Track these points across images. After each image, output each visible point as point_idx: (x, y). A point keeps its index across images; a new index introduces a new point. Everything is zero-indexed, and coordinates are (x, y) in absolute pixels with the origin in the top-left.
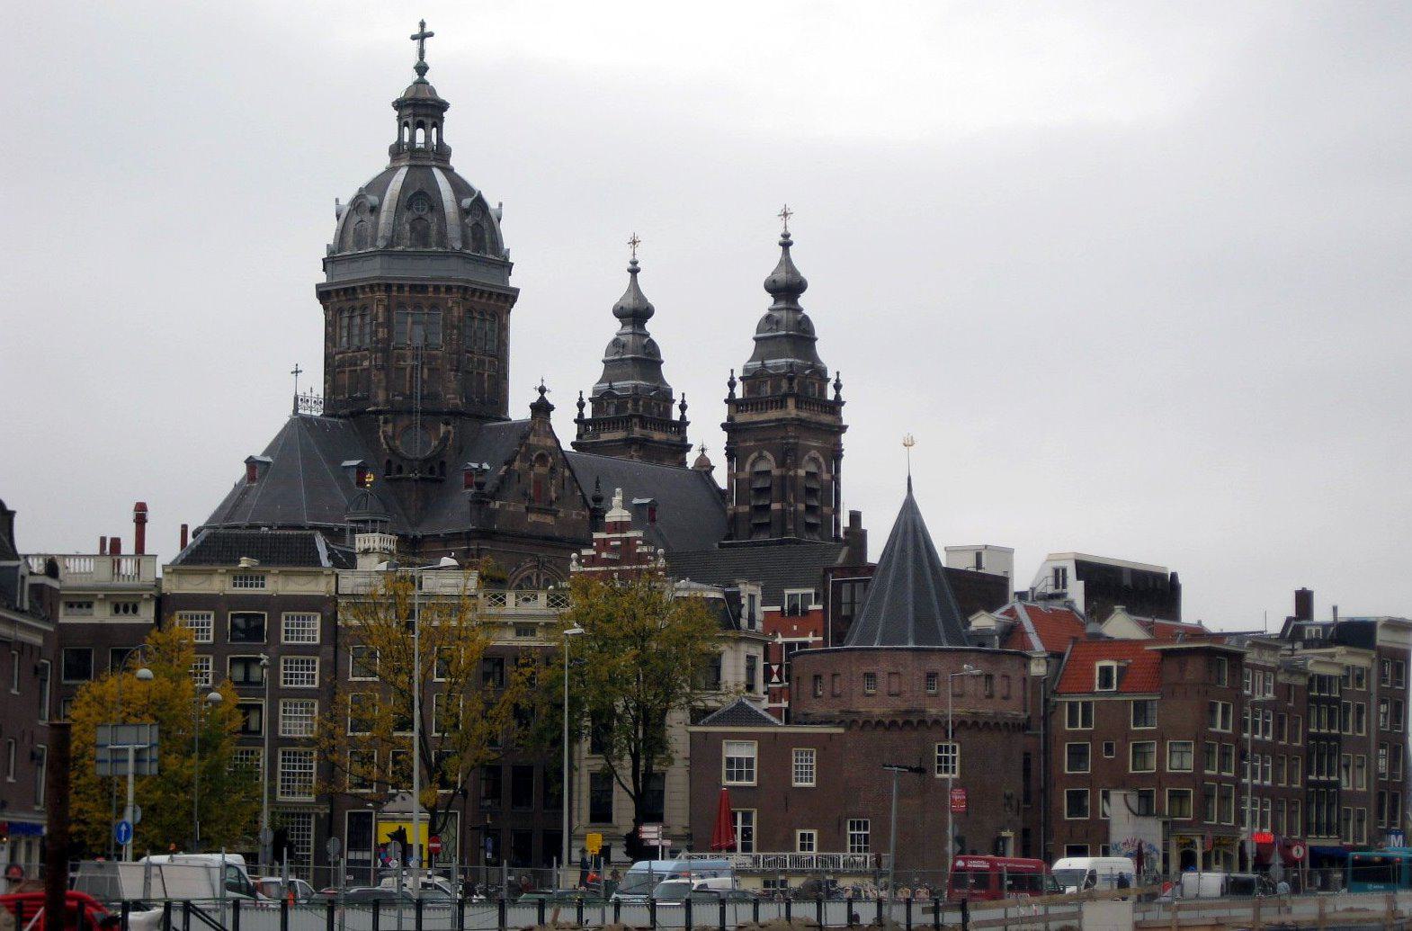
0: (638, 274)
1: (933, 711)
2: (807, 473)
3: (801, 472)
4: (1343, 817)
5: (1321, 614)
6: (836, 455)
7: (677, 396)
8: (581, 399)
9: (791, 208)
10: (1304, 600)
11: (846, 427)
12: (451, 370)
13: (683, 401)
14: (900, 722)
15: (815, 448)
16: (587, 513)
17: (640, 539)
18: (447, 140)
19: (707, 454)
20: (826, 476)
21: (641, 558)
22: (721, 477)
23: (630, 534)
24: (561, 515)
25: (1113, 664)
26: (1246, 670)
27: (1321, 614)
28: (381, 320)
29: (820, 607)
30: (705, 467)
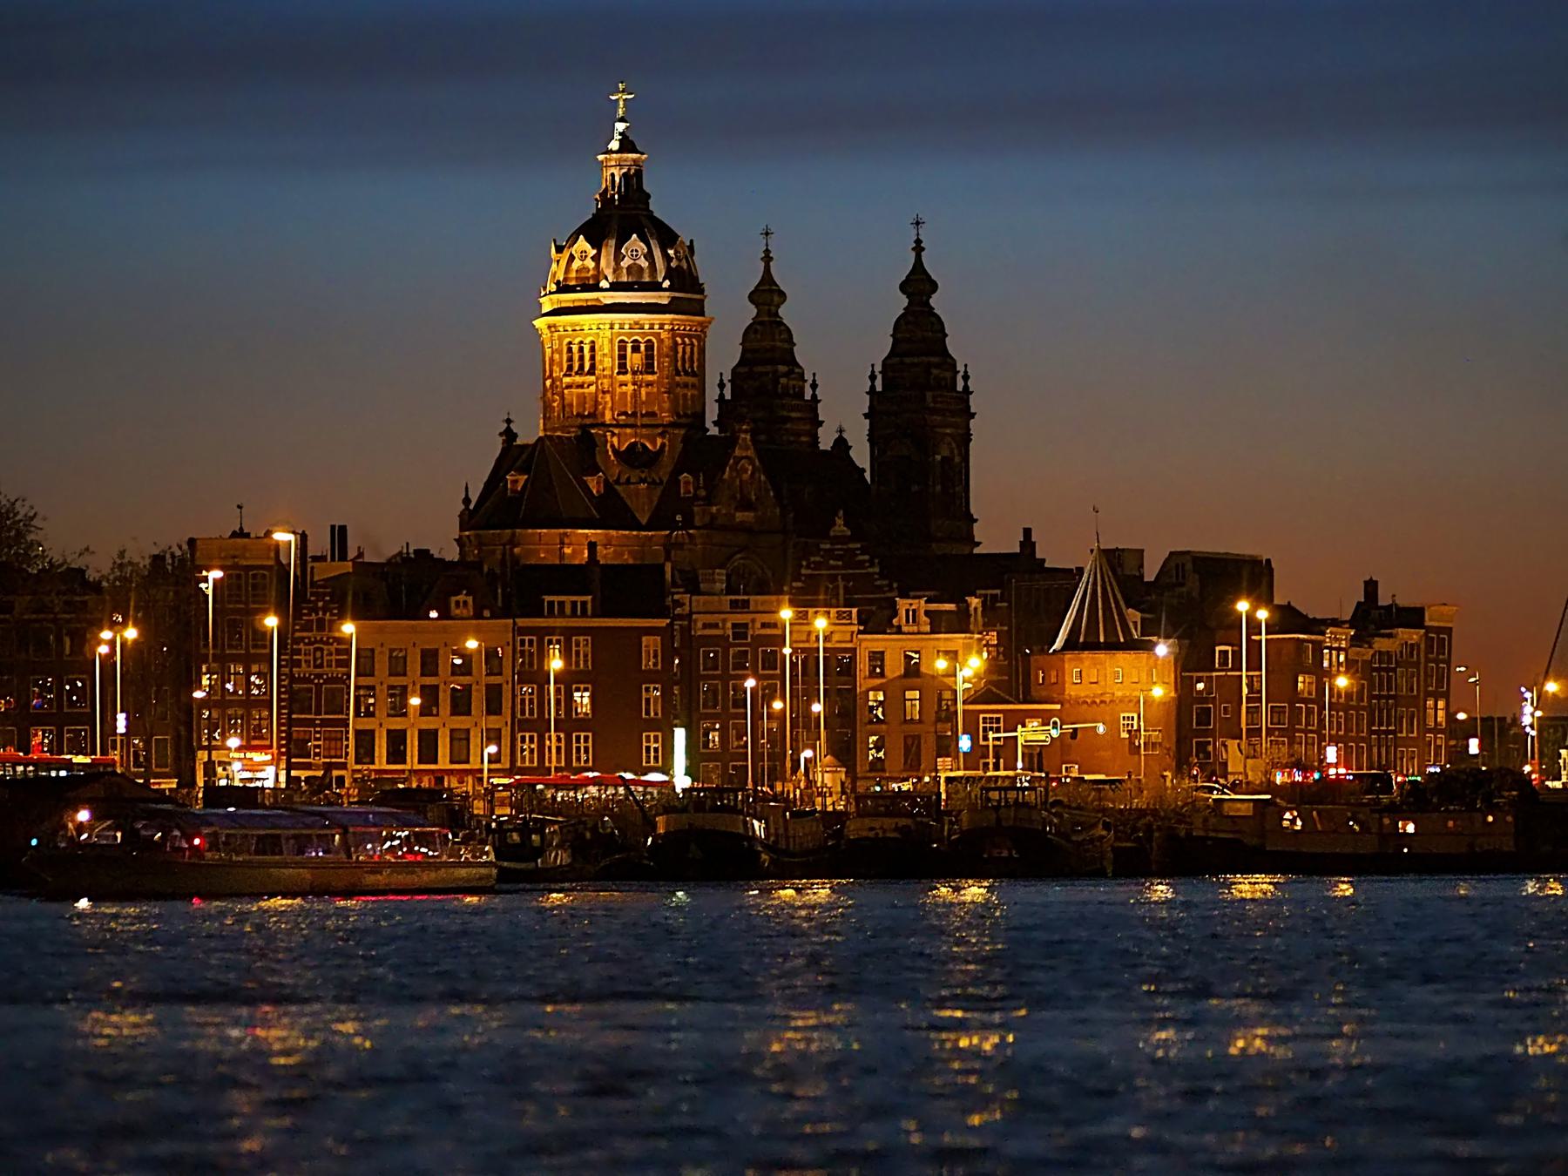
0: (771, 264)
1: (1119, 694)
2: (943, 458)
3: (938, 457)
4: (1399, 755)
5: (1383, 601)
6: (967, 438)
7: (808, 377)
8: (721, 380)
9: (924, 217)
10: (1371, 587)
11: (975, 414)
12: (665, 392)
13: (814, 381)
14: (1098, 701)
15: (947, 434)
16: (778, 510)
17: (857, 549)
18: (646, 187)
19: (845, 435)
20: (957, 459)
21: (861, 564)
22: (861, 455)
23: (851, 546)
24: (760, 513)
25: (1229, 648)
26: (1326, 651)
27: (1383, 601)
28: (606, 351)
29: (1005, 604)
30: (841, 444)
